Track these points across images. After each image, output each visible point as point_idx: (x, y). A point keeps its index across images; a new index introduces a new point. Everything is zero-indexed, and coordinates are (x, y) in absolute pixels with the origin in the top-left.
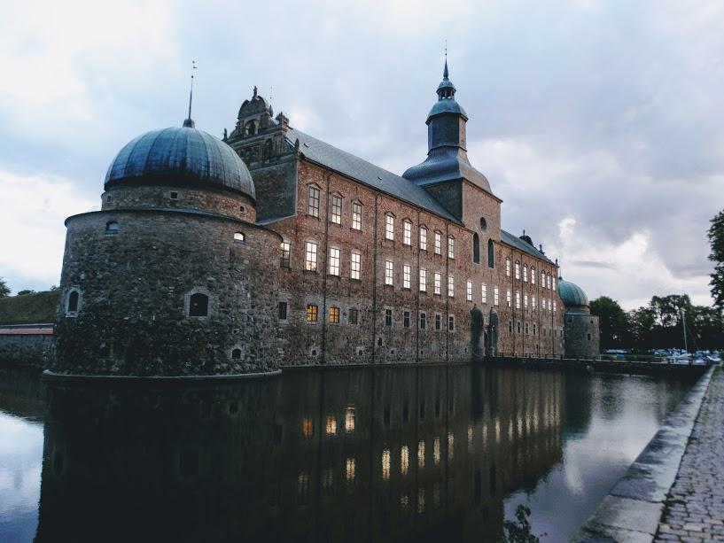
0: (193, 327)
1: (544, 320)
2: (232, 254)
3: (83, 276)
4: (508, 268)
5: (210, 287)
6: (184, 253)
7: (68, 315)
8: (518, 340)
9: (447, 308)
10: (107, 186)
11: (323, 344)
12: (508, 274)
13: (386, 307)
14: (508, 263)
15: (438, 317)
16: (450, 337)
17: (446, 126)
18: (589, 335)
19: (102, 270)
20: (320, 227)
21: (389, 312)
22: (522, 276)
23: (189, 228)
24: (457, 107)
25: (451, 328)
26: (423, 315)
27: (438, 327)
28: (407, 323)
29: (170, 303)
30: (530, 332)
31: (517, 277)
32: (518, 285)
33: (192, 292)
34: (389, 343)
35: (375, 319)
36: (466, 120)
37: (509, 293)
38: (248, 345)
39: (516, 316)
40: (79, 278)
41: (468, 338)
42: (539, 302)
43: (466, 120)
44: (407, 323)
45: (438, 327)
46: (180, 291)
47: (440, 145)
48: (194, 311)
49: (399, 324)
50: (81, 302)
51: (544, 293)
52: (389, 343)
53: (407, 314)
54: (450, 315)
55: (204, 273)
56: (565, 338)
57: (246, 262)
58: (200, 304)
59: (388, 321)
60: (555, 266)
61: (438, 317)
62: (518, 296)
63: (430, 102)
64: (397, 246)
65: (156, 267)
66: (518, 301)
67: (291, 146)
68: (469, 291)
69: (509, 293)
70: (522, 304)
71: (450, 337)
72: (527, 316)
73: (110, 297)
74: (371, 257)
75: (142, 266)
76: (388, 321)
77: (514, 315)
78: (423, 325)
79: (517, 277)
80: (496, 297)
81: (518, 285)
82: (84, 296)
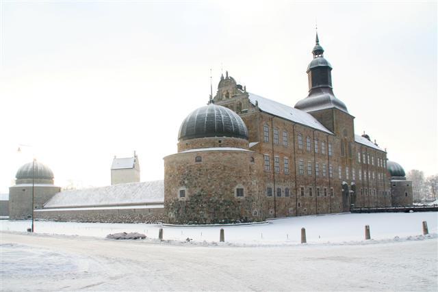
0: (239, 202)
1: (380, 186)
2: (250, 168)
3: (186, 182)
4: (359, 157)
5: (244, 183)
6: (232, 169)
7: (180, 199)
8: (366, 199)
9: (329, 184)
10: (179, 139)
11: (275, 208)
12: (359, 161)
13: (301, 186)
14: (359, 154)
15: (325, 189)
16: (332, 200)
17: (320, 76)
18: (406, 194)
19: (196, 179)
20: (270, 146)
21: (302, 189)
22: (367, 161)
23: (234, 157)
24: (325, 62)
25: (332, 195)
26: (318, 189)
27: (325, 195)
28: (311, 195)
29: (229, 192)
30: (372, 194)
31: (364, 162)
32: (365, 167)
33: (237, 187)
34: (304, 205)
35: (296, 193)
36: (331, 69)
37: (360, 173)
38: (259, 210)
39: (365, 185)
40: (184, 182)
41: (341, 200)
42: (376, 175)
43: (331, 69)
44: (311, 195)
45: (325, 195)
46: (232, 186)
47: (317, 86)
48: (238, 195)
49: (307, 195)
50: (187, 194)
51: (380, 170)
52: (304, 205)
53: (311, 189)
54: (332, 188)
55: (240, 177)
56: (392, 196)
57: (255, 171)
58: (240, 192)
59: (303, 194)
60: (384, 154)
61: (325, 189)
62: (365, 173)
63: (310, 58)
64: (304, 152)
65: (221, 176)
66: (365, 176)
67: (253, 105)
68: (340, 173)
69: (360, 173)
70: (367, 177)
71: (332, 200)
72: (370, 185)
73: (202, 190)
74: (293, 160)
75: (215, 176)
76: (303, 194)
77: (363, 185)
78: (318, 195)
79: (364, 162)
80: (354, 175)
81: (365, 167)
82: (189, 191)
